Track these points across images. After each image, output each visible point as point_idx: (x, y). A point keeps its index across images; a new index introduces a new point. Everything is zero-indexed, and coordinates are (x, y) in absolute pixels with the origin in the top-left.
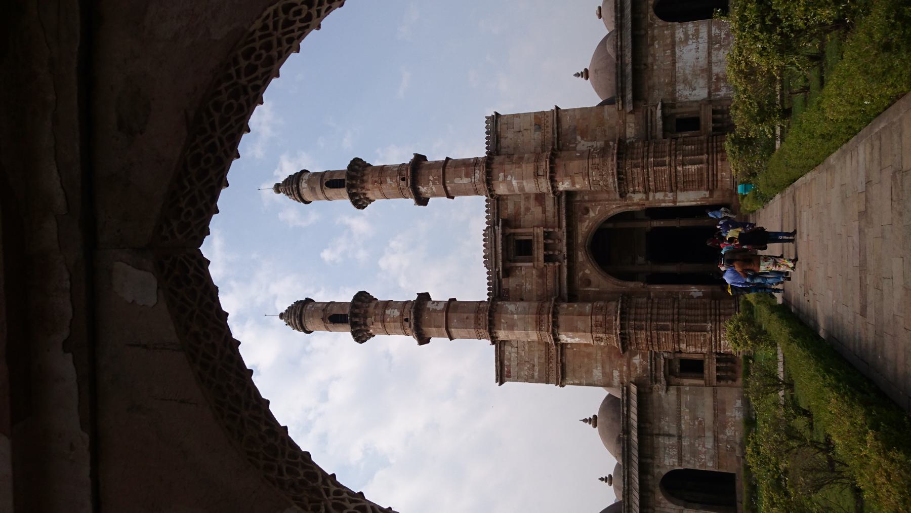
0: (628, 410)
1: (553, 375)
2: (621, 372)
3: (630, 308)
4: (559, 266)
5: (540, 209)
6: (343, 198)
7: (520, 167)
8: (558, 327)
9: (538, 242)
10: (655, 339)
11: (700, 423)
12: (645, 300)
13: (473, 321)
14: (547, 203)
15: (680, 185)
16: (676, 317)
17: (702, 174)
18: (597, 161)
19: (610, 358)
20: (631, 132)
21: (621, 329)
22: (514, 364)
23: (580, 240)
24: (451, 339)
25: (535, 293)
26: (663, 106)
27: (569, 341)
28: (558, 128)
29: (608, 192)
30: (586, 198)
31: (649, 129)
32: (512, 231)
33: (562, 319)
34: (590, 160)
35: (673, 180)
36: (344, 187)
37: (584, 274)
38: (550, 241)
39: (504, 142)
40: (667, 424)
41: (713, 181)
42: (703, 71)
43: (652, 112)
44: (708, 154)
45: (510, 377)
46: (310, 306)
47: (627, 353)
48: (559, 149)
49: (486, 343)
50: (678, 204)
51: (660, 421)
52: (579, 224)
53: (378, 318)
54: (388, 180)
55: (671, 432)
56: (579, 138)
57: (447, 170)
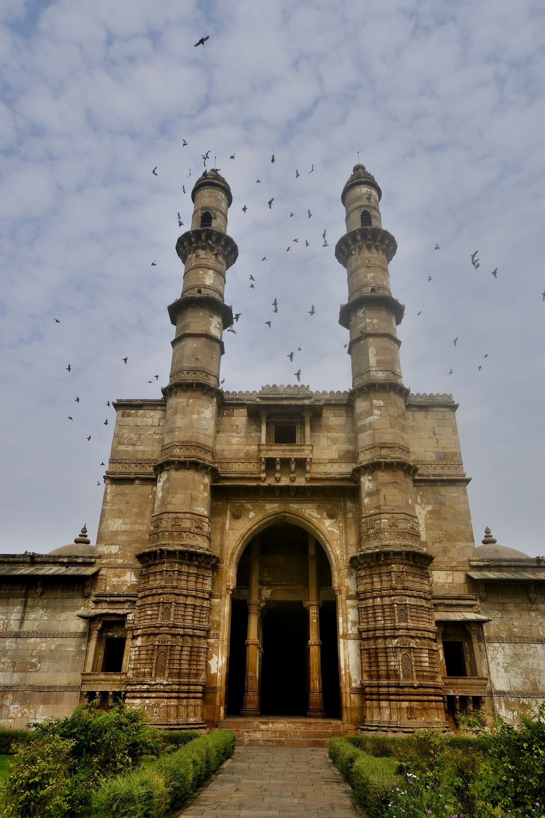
0: (62, 564)
1: (119, 468)
2: (116, 556)
3: (198, 567)
4: (259, 479)
5: (335, 456)
6: (348, 229)
7: (392, 426)
8: (177, 470)
9: (293, 450)
10: (150, 600)
11: (34, 665)
12: (208, 588)
13: (192, 365)
14: (344, 465)
15: (371, 644)
16: (181, 631)
17: (388, 677)
18: (402, 525)
19: (136, 541)
20: (439, 577)
21: (169, 552)
22: (139, 421)
23: (294, 507)
24: (174, 343)
25: (226, 447)
26: (480, 623)
27: (160, 485)
28: (442, 481)
29: (360, 543)
30: (350, 515)
31: (446, 602)
32: (307, 420)
33: (189, 474)
34: (403, 516)
35: (379, 633)
36: (362, 226)
37: (249, 510)
38: (293, 467)
39: (420, 415)
40: (38, 617)
41: (379, 694)
42: (535, 684)
43: (471, 606)
44: (418, 687)
45: (123, 416)
46: (222, 195)
47: (139, 565)
48: (415, 481)
49: (166, 382)
50: (341, 641)
51: (43, 608)
52: (315, 505)
53: (203, 262)
54: (372, 275)
55: (26, 623)
56: (430, 508)
57: (386, 339)
